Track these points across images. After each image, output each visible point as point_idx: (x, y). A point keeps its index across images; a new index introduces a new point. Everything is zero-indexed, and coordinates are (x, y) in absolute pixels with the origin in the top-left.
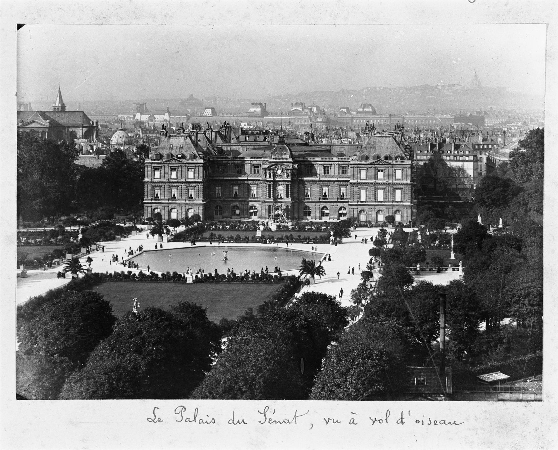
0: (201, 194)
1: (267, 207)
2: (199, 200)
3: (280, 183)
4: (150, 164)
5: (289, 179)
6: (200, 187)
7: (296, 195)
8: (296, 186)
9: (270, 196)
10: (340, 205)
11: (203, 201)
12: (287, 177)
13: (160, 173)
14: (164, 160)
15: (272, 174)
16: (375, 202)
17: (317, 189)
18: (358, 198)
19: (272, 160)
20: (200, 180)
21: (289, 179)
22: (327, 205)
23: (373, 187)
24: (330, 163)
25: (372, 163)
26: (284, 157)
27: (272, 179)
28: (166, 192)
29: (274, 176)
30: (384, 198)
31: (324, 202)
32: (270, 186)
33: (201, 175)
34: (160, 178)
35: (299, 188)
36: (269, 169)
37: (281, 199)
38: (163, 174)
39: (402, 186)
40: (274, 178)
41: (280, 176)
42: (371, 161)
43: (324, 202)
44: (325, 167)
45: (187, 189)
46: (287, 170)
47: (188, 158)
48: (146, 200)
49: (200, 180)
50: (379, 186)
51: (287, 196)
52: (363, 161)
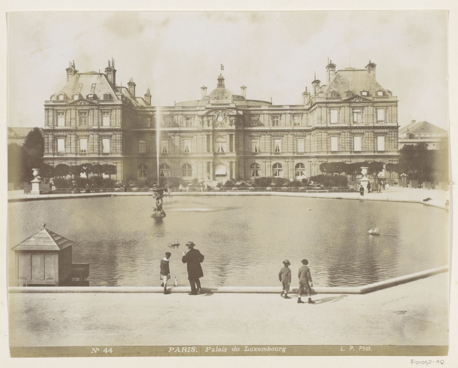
0: (119, 146)
1: (205, 165)
2: (117, 153)
3: (221, 134)
4: (51, 108)
5: (234, 127)
6: (118, 136)
7: (241, 149)
8: (241, 137)
9: (208, 151)
10: (299, 161)
11: (122, 154)
12: (231, 125)
13: (65, 119)
14: (69, 102)
15: (211, 122)
16: (351, 152)
17: (268, 142)
18: (327, 148)
19: (210, 106)
20: (118, 126)
21: (234, 127)
22: (281, 162)
23: (347, 133)
24: (280, 112)
25: (345, 101)
26: (225, 101)
27: (211, 128)
28: (73, 144)
29: (214, 125)
30: (362, 147)
31: (276, 157)
32: (208, 136)
33: (119, 120)
34: (65, 125)
35: (244, 140)
36: (207, 115)
37: (223, 153)
38: (68, 120)
39: (386, 131)
40: (213, 127)
41: (222, 124)
42: (344, 98)
43: (276, 157)
44: (273, 118)
45: (100, 138)
46: (230, 116)
47: (102, 98)
48: (46, 154)
49: (118, 126)
50: (355, 131)
51: (231, 150)
52: (334, 99)
